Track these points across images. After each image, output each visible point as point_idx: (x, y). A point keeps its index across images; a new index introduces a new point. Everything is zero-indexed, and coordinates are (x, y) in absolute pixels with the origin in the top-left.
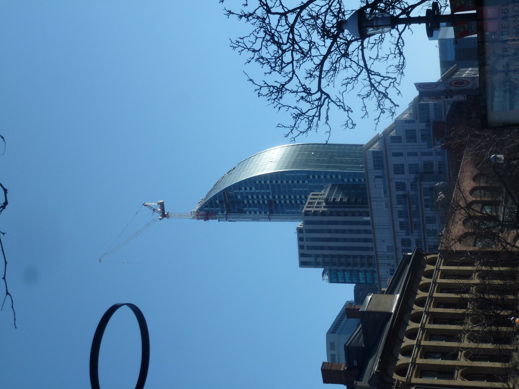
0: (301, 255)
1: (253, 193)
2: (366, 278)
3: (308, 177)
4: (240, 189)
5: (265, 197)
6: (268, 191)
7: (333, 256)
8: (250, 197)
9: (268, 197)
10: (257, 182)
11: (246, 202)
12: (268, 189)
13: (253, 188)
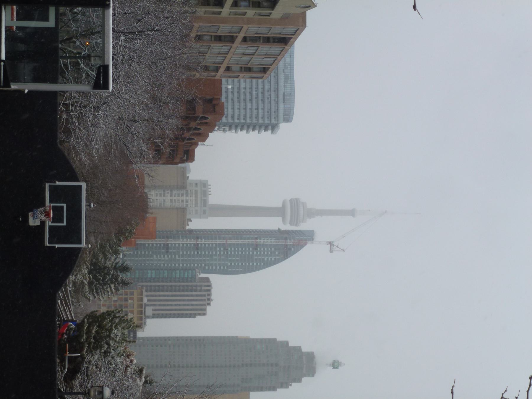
0: (209, 290)
1: (267, 255)
2: (176, 273)
3: (227, 267)
4: (275, 259)
5: (259, 253)
6: (256, 257)
7: (191, 291)
8: (269, 253)
9: (257, 253)
10: (262, 264)
11: (273, 249)
12: (256, 259)
13: (266, 259)
